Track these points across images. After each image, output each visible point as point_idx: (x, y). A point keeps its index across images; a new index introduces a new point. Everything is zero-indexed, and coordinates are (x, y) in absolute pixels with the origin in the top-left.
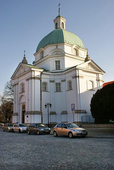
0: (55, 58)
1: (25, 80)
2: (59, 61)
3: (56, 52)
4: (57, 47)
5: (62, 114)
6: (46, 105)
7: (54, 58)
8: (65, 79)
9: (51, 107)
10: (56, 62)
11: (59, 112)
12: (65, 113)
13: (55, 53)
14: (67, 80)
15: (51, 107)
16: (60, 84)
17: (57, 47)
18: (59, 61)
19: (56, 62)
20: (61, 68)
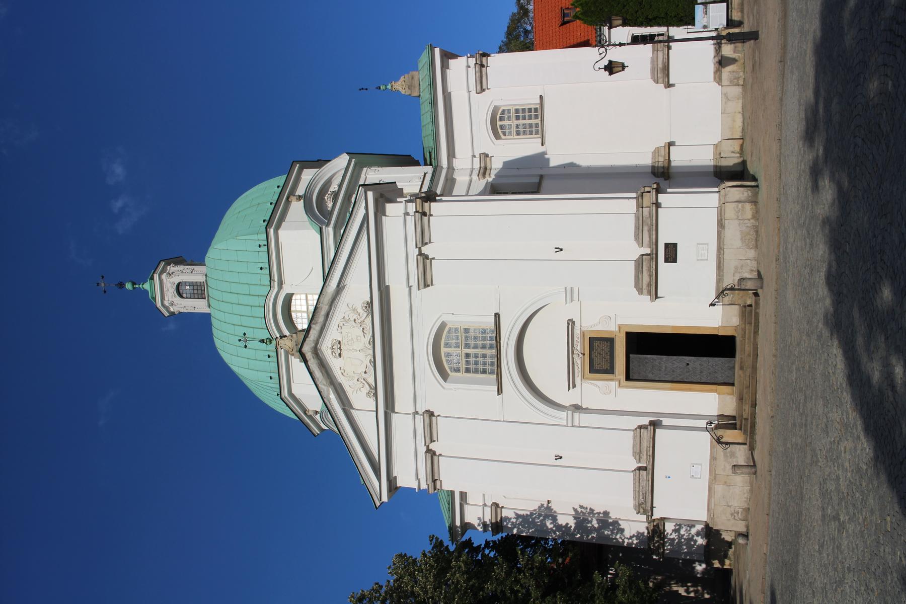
6: (611, 68)
8: (477, 160)
14: (486, 142)
17: (299, 198)
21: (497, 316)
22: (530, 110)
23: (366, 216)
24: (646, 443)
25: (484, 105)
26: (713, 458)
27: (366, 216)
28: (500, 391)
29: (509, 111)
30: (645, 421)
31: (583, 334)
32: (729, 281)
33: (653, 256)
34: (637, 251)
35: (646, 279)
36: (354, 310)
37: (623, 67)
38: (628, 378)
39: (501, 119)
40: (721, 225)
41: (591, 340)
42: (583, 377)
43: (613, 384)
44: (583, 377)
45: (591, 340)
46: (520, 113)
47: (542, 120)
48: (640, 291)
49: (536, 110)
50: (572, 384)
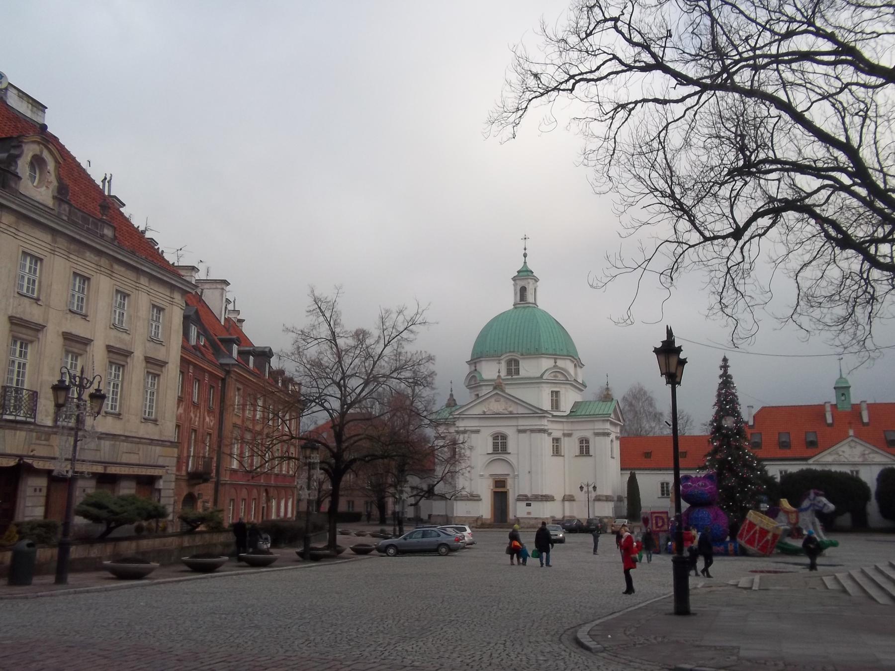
0: (553, 385)
1: (515, 428)
2: (557, 393)
3: (554, 374)
4: (555, 363)
5: (564, 500)
6: (581, 488)
7: (549, 385)
8: (570, 432)
9: (595, 491)
10: (552, 392)
11: (558, 497)
12: (569, 498)
13: (552, 375)
14: (577, 435)
15: (595, 491)
16: (556, 440)
17: (555, 363)
18: (557, 393)
19: (552, 392)
20: (562, 408)
21: (510, 453)
22: (589, 451)
23: (538, 413)
24: (476, 498)
25: (588, 434)
26: (472, 517)
27: (538, 413)
28: (488, 454)
29: (588, 443)
30: (481, 497)
31: (506, 479)
32: (521, 521)
33: (528, 499)
34: (529, 495)
35: (521, 497)
36: (510, 407)
37: (582, 491)
38: (495, 493)
39: (586, 440)
40: (536, 518)
41: (504, 481)
42: (494, 479)
43: (492, 488)
44: (494, 479)
45: (504, 481)
46: (588, 448)
47: (585, 456)
48: (518, 496)
49: (589, 453)
50: (491, 475)
